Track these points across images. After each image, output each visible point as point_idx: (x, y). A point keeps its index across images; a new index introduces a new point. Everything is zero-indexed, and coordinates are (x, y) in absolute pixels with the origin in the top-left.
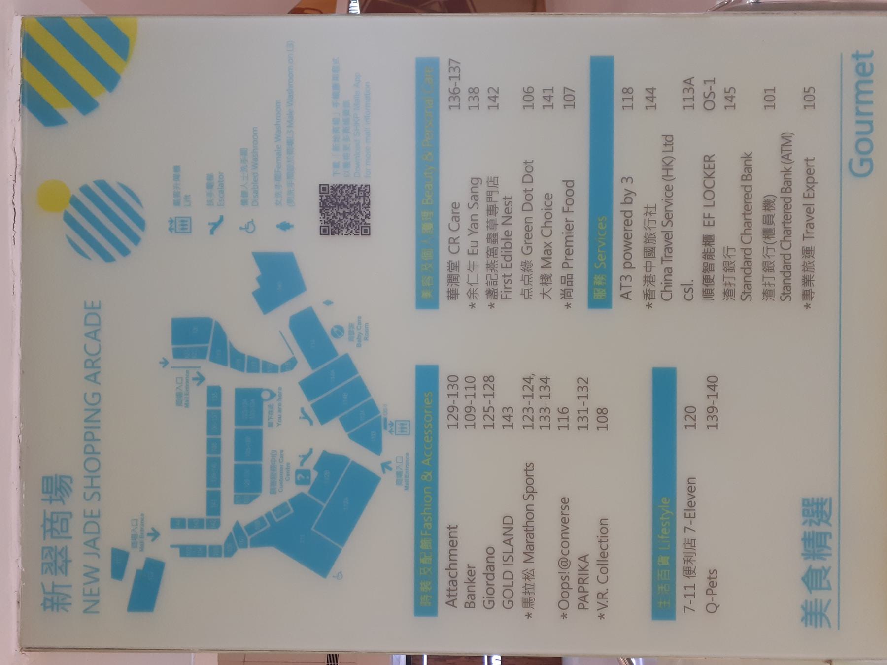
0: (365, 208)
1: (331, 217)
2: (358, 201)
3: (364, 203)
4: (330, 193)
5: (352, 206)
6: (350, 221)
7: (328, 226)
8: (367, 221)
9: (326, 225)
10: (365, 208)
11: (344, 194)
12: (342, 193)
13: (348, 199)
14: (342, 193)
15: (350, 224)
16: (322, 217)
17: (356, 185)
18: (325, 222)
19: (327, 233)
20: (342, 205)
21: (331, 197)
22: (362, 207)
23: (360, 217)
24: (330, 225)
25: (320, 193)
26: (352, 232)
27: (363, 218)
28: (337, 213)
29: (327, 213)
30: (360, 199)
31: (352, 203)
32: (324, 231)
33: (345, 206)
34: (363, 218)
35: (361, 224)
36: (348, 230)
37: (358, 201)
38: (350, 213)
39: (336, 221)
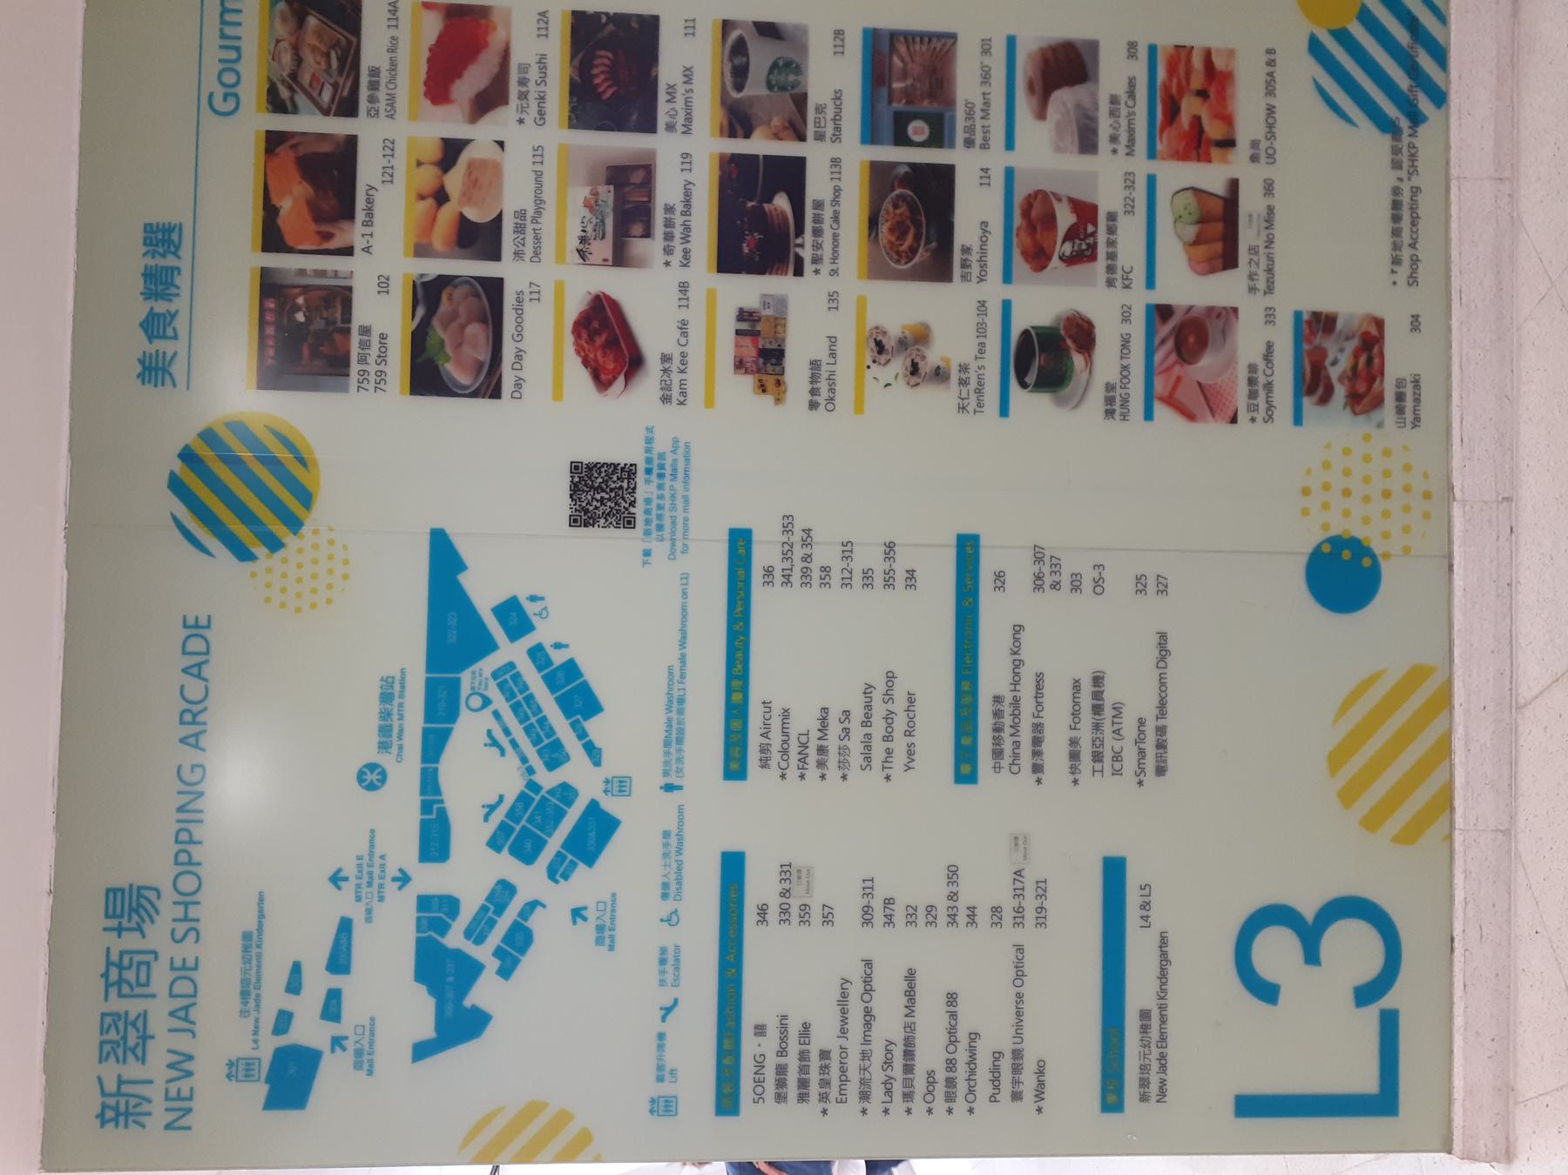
0: (630, 493)
1: (584, 504)
2: (620, 483)
3: (629, 487)
4: (584, 474)
5: (612, 490)
6: (609, 510)
7: (581, 516)
8: (632, 510)
9: (578, 513)
10: (630, 493)
11: (603, 475)
12: (599, 474)
13: (607, 481)
14: (599, 474)
15: (609, 514)
16: (572, 503)
17: (619, 464)
18: (576, 510)
19: (579, 524)
20: (599, 489)
21: (586, 479)
22: (625, 492)
23: (623, 504)
24: (582, 514)
25: (571, 472)
26: (611, 523)
27: (627, 505)
28: (592, 498)
29: (580, 498)
30: (622, 482)
31: (613, 486)
32: (574, 522)
33: (603, 491)
34: (627, 505)
35: (624, 513)
36: (607, 520)
37: (620, 483)
38: (609, 500)
39: (591, 508)
